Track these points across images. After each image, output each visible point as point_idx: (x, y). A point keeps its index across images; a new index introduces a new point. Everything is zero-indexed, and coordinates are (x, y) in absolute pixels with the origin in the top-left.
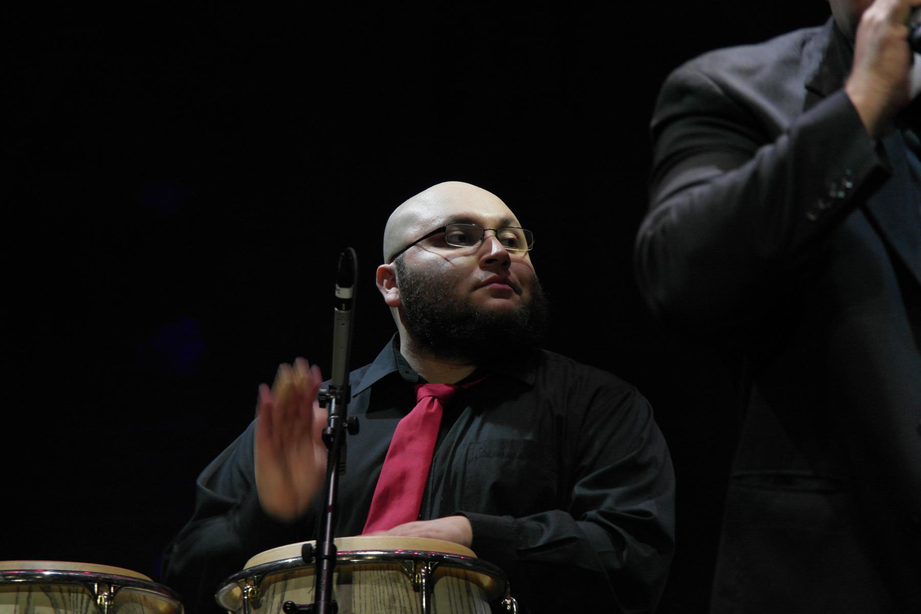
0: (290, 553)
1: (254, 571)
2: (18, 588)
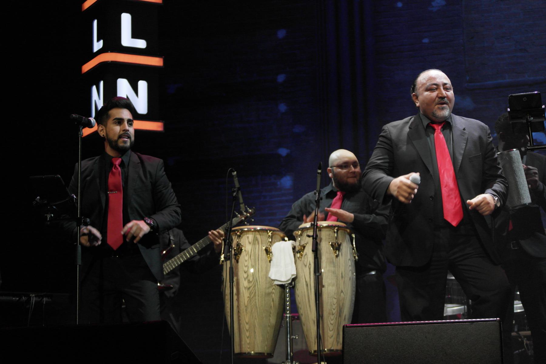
1: (301, 228)
2: (253, 231)
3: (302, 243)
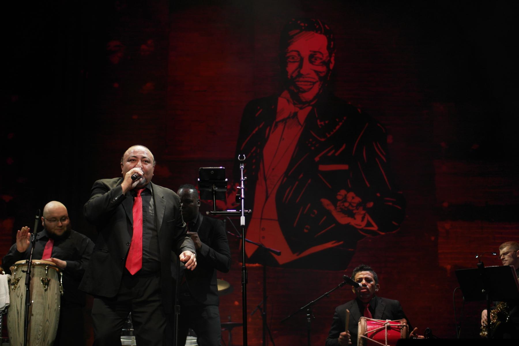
0: (23, 262)
3: (17, 277)
